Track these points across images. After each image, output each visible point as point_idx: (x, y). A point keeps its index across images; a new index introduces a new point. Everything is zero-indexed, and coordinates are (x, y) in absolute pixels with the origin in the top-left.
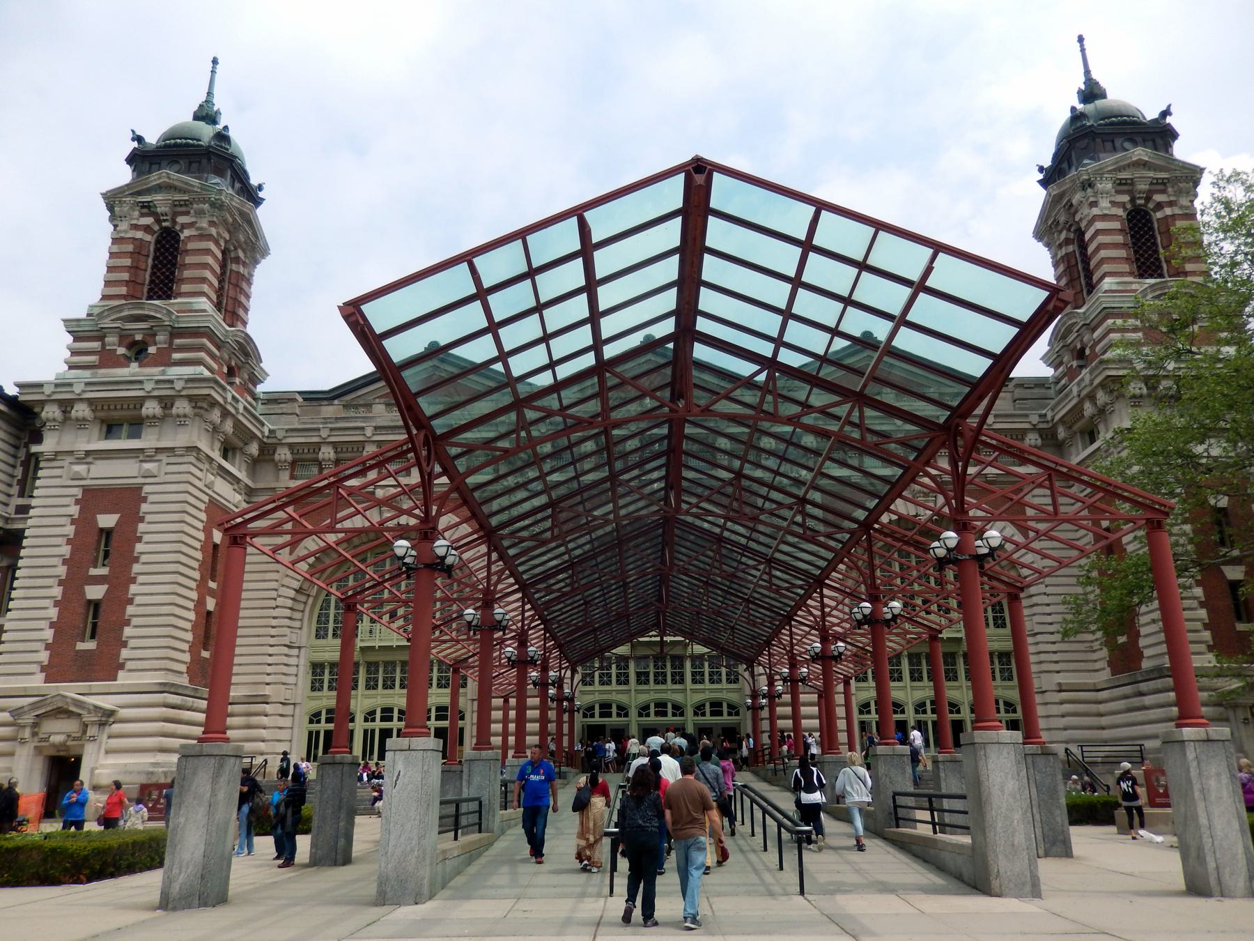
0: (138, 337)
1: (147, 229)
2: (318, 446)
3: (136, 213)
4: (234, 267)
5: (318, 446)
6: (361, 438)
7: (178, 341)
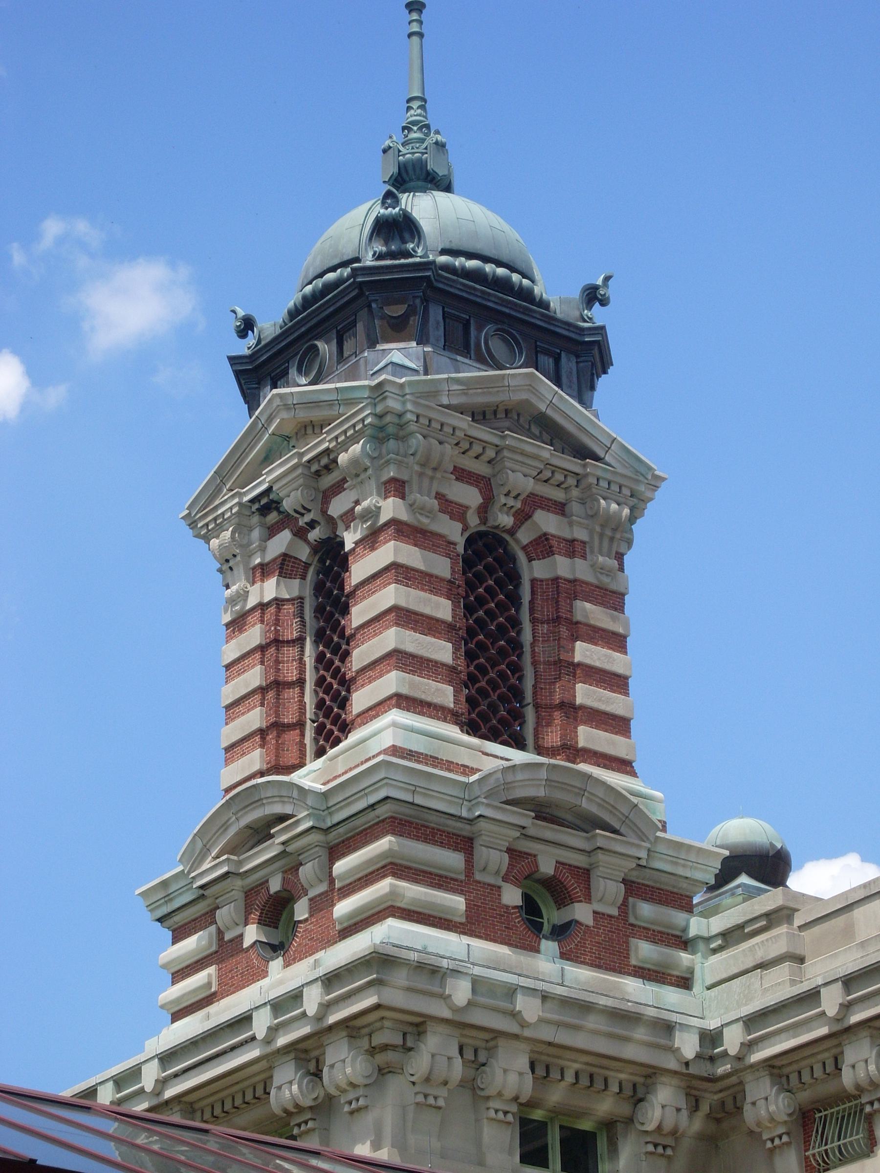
0: (275, 885)
1: (285, 566)
3: (256, 534)
4: (540, 569)
7: (341, 866)
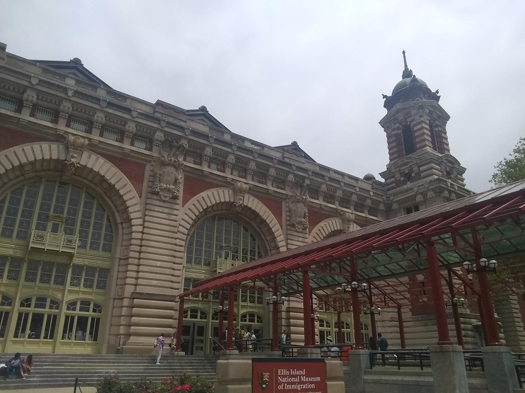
2: (25, 89)
5: (25, 89)
6: (63, 95)
